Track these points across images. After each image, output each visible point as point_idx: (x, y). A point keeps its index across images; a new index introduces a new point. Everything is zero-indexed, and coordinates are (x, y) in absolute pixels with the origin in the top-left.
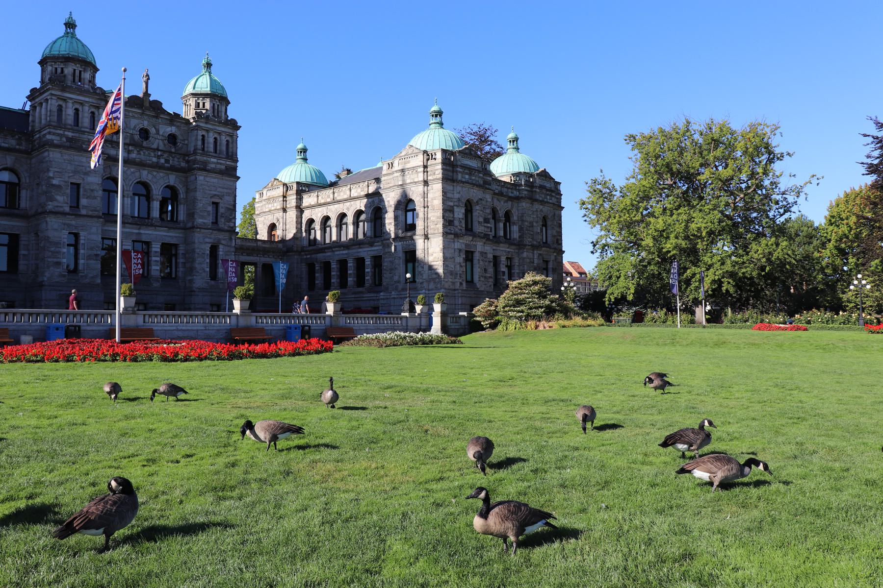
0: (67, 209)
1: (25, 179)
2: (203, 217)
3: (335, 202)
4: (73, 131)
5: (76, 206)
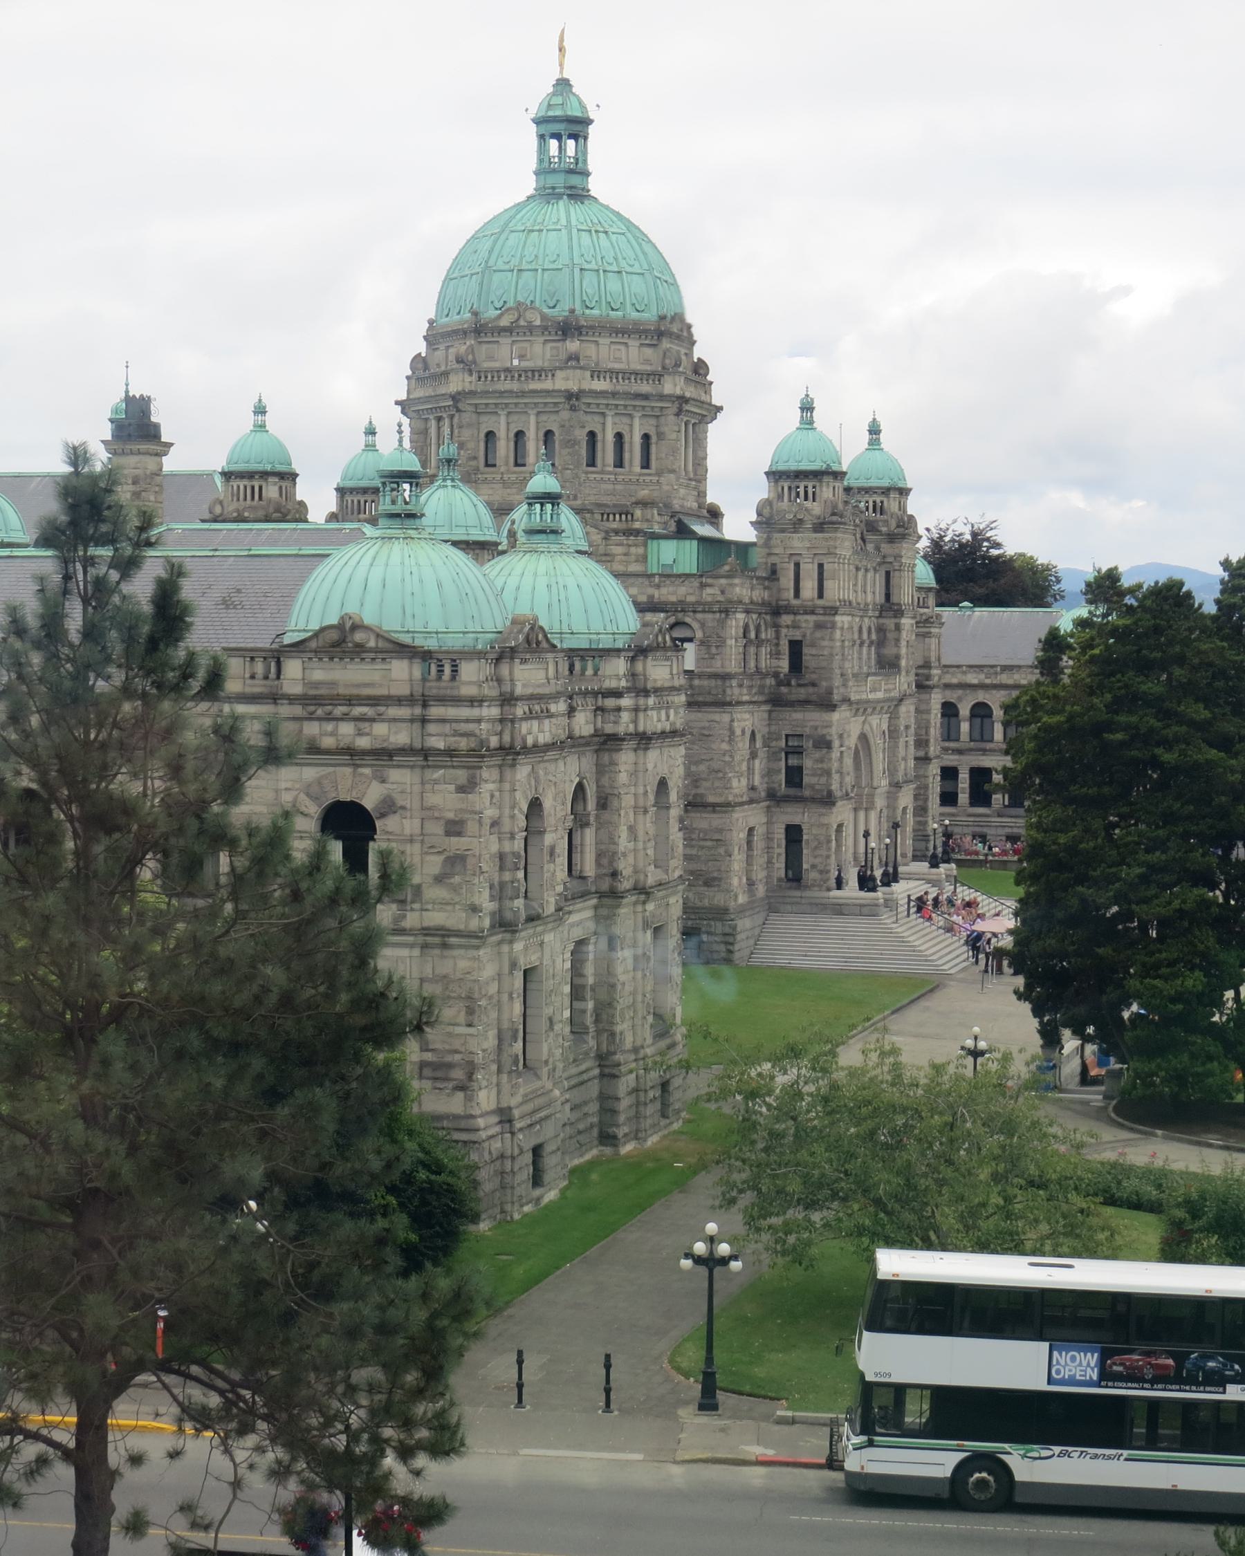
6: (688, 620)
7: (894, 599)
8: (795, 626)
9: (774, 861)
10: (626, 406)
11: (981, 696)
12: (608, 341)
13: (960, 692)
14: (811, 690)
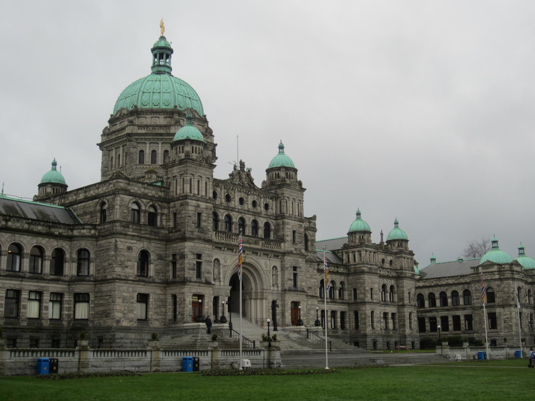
0: (370, 300)
1: (346, 286)
3: (437, 286)
6: (105, 200)
7: (282, 212)
8: (175, 207)
9: (168, 311)
10: (154, 139)
11: (454, 288)
12: (150, 116)
13: (447, 287)
14: (179, 233)
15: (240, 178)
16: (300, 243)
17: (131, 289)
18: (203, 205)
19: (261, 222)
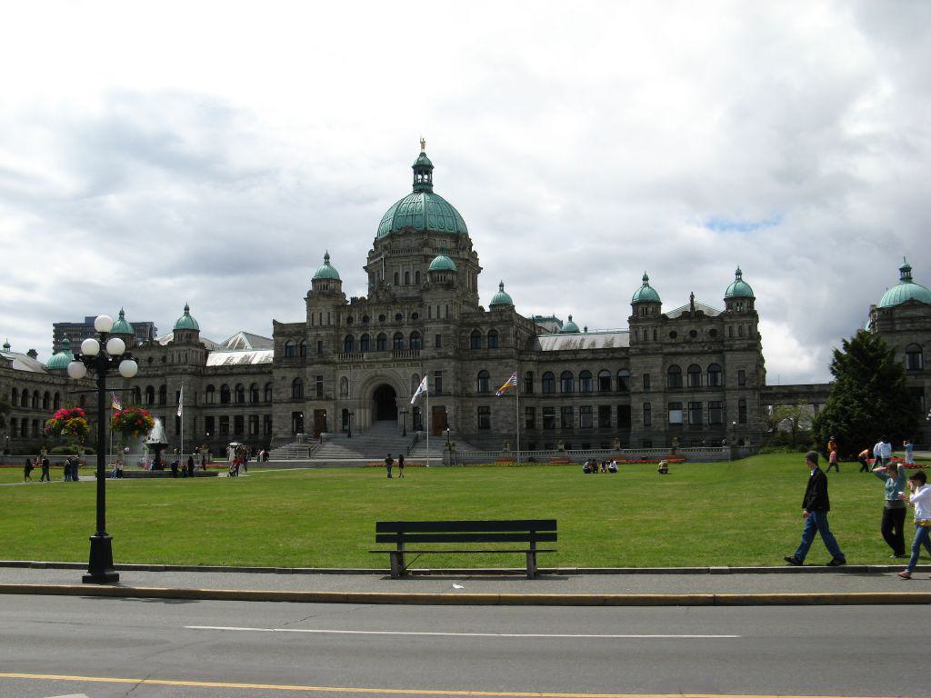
0: (642, 390)
2: (731, 382)
4: (643, 344)
5: (646, 386)
15: (378, 297)
16: (446, 346)
17: (285, 410)
18: (323, 333)
19: (407, 331)
